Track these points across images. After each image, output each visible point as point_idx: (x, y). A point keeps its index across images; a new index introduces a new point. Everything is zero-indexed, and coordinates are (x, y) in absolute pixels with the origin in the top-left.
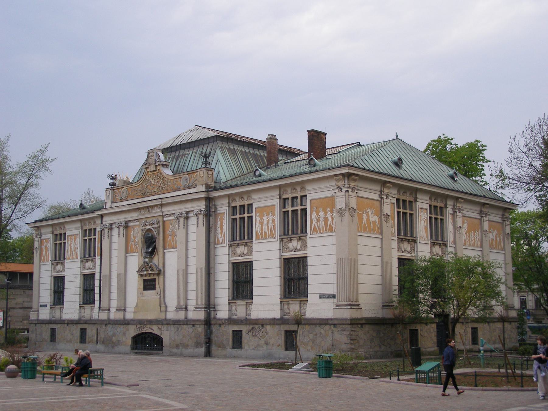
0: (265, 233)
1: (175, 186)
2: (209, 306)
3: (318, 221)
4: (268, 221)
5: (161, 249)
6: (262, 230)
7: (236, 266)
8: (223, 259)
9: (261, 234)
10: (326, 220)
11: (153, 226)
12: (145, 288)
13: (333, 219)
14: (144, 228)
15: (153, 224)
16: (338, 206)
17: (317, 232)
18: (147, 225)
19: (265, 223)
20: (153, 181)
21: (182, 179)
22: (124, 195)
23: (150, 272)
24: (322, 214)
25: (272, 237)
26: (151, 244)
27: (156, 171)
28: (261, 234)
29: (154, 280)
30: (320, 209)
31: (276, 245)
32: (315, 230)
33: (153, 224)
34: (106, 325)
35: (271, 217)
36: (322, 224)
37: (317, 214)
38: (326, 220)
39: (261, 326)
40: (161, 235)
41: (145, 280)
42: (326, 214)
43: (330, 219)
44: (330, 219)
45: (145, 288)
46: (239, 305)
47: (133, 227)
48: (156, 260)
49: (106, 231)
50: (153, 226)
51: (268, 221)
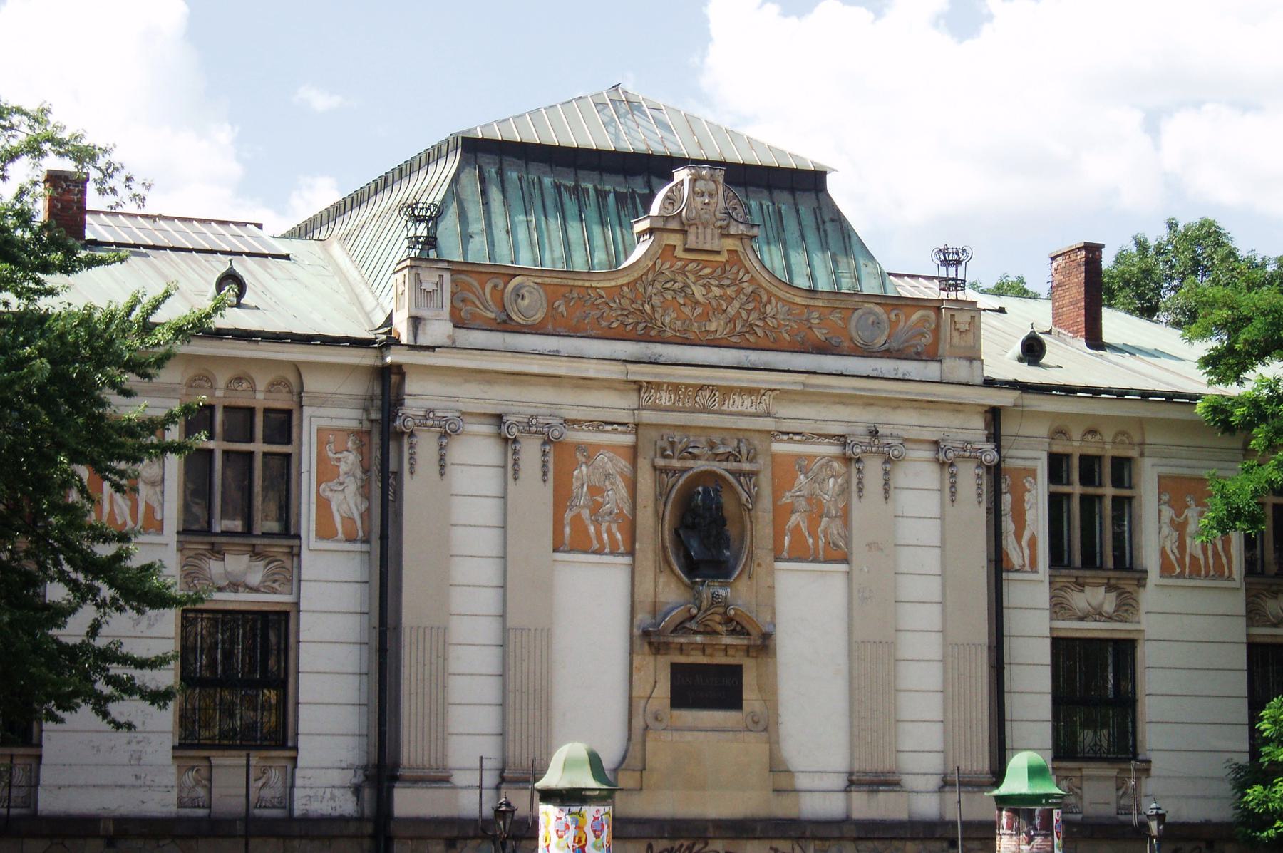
0: (1193, 558)
1: (820, 334)
5: (763, 554)
6: (1182, 546)
7: (1067, 652)
9: (1181, 561)
11: (733, 465)
14: (676, 463)
15: (728, 457)
18: (695, 457)
20: (698, 292)
21: (857, 314)
23: (728, 640)
25: (1220, 574)
26: (704, 531)
27: (718, 253)
28: (1181, 561)
29: (737, 671)
31: (1237, 603)
33: (728, 457)
34: (451, 843)
39: (1203, 845)
40: (766, 503)
41: (676, 669)
46: (1090, 778)
47: (589, 452)
48: (739, 594)
49: (426, 446)
50: (733, 465)
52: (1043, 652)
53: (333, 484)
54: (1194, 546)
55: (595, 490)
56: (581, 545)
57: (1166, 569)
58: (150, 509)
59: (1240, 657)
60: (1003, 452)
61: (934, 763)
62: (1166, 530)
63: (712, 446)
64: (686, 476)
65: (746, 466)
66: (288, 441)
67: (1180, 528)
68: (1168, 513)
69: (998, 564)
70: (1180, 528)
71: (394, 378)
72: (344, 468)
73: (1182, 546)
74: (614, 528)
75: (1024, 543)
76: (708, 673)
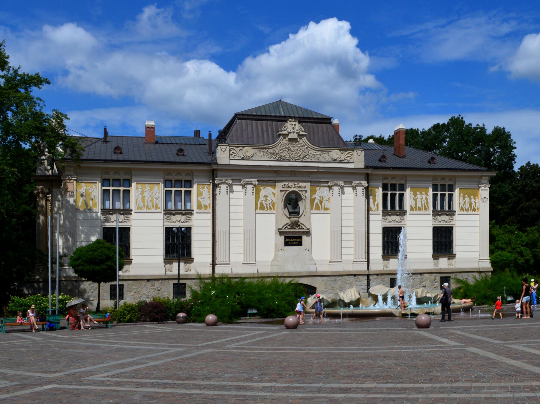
2: (368, 261)
3: (465, 203)
4: (422, 199)
6: (416, 204)
8: (378, 223)
9: (416, 208)
10: (471, 204)
12: (287, 244)
13: (476, 203)
16: (483, 196)
17: (463, 211)
18: (291, 188)
19: (419, 200)
20: (292, 149)
22: (249, 154)
24: (467, 199)
28: (416, 208)
29: (301, 238)
30: (466, 196)
32: (462, 209)
35: (424, 196)
36: (467, 206)
37: (464, 198)
38: (471, 204)
41: (286, 237)
42: (470, 199)
43: (474, 204)
44: (474, 204)
45: (287, 244)
51: (422, 199)
52: (380, 231)
53: (201, 197)
54: (419, 205)
55: (266, 196)
56: (262, 208)
57: (412, 209)
58: (157, 204)
59: (431, 231)
60: (370, 184)
61: (352, 258)
62: (412, 200)
63: (295, 185)
64: (287, 192)
65: (303, 189)
66: (191, 188)
67: (416, 200)
68: (413, 196)
69: (368, 209)
70: (416, 200)
71: (215, 172)
72: (204, 192)
73: (416, 204)
74: (271, 205)
75: (376, 205)
76: (293, 238)
